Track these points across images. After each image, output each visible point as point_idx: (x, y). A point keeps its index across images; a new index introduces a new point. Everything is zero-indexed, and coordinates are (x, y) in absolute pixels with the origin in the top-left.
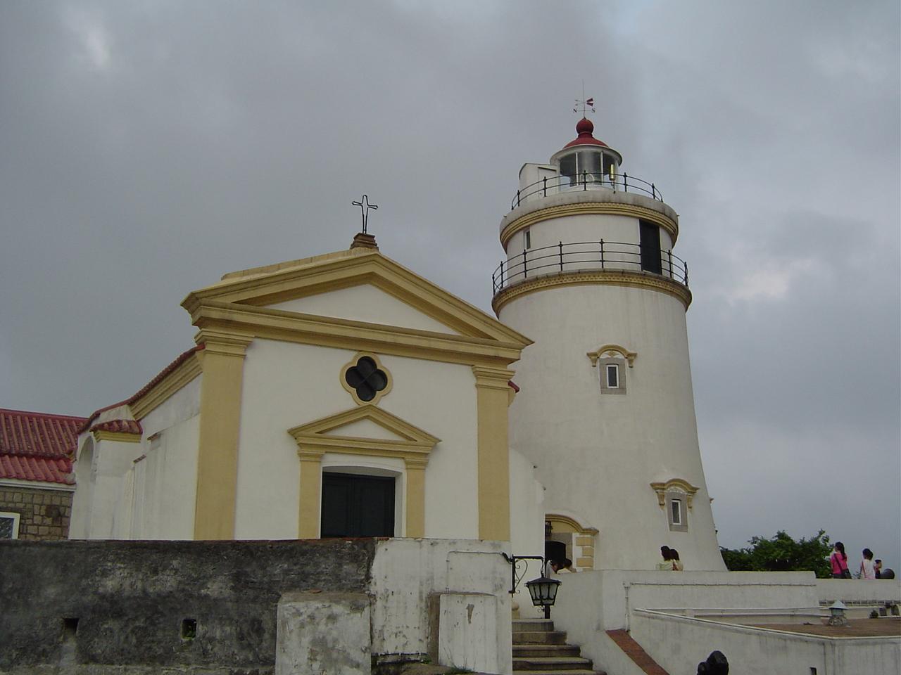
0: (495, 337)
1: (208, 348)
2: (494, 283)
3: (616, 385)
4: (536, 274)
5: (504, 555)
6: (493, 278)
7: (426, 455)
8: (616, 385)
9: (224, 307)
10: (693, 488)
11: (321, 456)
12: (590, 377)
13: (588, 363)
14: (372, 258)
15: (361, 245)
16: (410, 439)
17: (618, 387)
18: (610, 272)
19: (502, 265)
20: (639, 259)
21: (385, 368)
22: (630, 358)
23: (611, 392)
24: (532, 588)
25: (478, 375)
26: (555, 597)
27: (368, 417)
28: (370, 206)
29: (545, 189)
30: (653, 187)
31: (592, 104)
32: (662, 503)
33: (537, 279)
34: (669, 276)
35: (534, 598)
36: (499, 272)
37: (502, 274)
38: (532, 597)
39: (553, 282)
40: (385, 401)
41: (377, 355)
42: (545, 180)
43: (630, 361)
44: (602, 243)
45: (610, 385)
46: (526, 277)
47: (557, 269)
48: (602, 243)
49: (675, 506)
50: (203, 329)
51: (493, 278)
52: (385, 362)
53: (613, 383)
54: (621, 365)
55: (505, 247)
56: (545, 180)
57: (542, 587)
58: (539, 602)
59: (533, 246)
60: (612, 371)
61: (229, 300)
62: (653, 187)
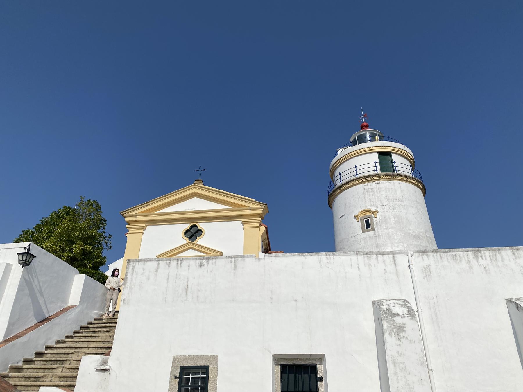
1: (130, 232)
9: (132, 216)
12: (358, 226)
17: (370, 228)
23: (368, 231)
25: (243, 224)
40: (200, 241)
45: (367, 228)
52: (201, 226)
53: (368, 226)
60: (367, 222)
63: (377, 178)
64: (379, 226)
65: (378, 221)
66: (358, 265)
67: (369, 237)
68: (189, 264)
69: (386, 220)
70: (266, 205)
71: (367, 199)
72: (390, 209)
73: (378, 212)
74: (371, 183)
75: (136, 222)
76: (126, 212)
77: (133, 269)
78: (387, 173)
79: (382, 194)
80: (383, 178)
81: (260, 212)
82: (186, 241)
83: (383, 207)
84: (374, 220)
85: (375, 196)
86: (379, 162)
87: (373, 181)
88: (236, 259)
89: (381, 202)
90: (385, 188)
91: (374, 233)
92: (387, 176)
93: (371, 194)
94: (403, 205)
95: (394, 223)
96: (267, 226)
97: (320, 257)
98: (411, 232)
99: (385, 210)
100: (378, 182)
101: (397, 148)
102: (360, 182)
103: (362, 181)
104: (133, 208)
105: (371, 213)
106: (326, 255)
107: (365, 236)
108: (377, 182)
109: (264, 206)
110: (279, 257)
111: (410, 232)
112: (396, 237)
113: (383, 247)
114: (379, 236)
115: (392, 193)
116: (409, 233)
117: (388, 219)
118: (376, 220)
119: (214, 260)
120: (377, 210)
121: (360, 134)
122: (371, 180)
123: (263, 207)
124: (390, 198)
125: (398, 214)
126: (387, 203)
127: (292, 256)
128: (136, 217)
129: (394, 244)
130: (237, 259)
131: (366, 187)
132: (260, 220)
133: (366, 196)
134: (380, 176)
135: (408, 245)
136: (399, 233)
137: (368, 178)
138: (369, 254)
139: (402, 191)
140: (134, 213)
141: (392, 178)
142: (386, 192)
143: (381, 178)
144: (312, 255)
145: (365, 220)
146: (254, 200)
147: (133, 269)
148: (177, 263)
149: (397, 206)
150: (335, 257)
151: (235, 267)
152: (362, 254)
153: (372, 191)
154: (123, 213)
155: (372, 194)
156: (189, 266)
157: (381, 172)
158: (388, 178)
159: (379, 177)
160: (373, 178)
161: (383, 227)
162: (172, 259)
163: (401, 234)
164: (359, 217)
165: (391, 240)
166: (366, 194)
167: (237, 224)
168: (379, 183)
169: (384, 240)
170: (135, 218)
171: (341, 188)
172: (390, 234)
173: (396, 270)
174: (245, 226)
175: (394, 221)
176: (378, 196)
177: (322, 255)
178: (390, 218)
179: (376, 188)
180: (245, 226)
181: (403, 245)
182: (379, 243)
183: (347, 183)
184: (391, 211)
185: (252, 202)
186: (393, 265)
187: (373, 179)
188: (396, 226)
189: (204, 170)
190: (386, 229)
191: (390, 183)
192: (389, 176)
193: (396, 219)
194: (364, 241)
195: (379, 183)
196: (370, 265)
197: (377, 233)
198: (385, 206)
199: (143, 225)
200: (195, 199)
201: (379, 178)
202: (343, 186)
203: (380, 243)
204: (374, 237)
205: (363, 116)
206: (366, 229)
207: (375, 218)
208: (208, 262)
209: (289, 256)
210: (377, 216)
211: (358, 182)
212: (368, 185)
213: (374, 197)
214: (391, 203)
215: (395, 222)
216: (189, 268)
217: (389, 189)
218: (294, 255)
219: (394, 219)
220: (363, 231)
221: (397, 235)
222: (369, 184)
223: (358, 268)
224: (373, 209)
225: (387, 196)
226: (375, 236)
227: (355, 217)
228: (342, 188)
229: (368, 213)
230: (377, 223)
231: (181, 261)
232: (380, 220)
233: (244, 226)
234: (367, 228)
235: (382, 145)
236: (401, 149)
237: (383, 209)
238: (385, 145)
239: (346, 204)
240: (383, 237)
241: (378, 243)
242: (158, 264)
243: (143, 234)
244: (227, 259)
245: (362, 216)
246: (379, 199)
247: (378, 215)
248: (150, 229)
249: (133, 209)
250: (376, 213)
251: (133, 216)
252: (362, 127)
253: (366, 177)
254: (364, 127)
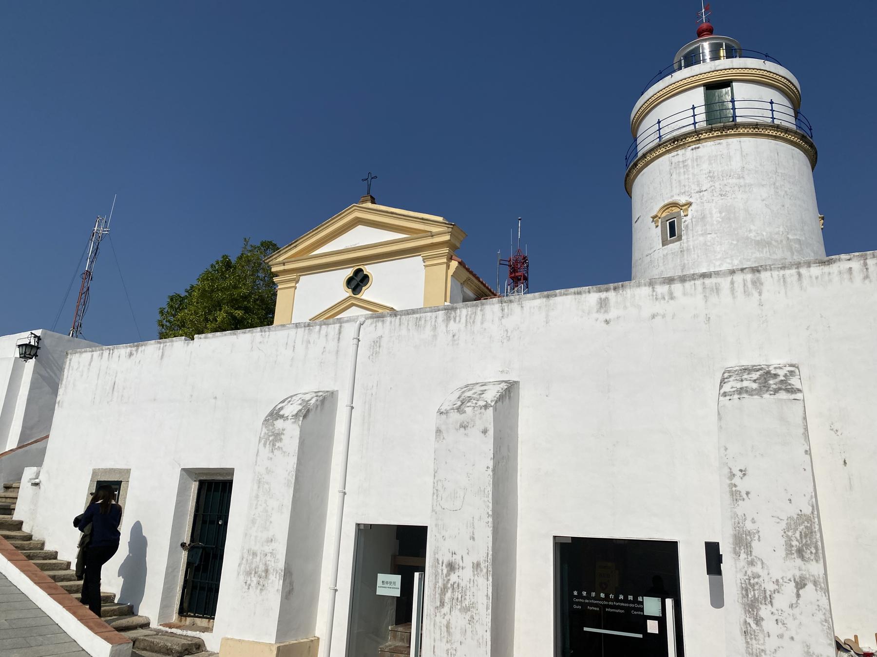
1: (279, 287)
23: (673, 242)
40: (367, 294)
45: (670, 238)
52: (368, 269)
53: (672, 234)
54: (678, 215)
60: (672, 225)
63: (694, 139)
64: (690, 232)
65: (690, 221)
66: (295, 343)
67: (672, 253)
68: (120, 354)
69: (703, 218)
70: (453, 225)
71: (674, 182)
72: (713, 195)
73: (690, 204)
74: (683, 151)
76: (271, 259)
77: (70, 363)
78: (713, 126)
79: (701, 168)
80: (707, 136)
81: (447, 238)
82: (348, 293)
83: (702, 194)
84: (683, 220)
85: (688, 175)
87: (687, 145)
88: (165, 344)
89: (698, 185)
90: (710, 157)
91: (681, 245)
92: (713, 132)
93: (682, 170)
94: (742, 184)
95: (719, 222)
96: (460, 260)
97: (254, 334)
98: (752, 235)
99: (705, 198)
100: (697, 146)
101: (746, 69)
102: (664, 150)
103: (668, 149)
104: (278, 252)
105: (679, 208)
106: (261, 331)
107: (665, 252)
108: (694, 146)
109: (452, 228)
110: (209, 338)
111: (749, 235)
112: (718, 249)
113: (693, 269)
114: (688, 250)
115: (721, 164)
116: (747, 238)
117: (709, 216)
118: (687, 220)
119: (143, 347)
120: (691, 200)
121: (688, 50)
122: (684, 144)
123: (450, 230)
124: (716, 174)
125: (728, 204)
126: (709, 186)
127: (223, 336)
128: (284, 265)
129: (714, 261)
130: (166, 344)
131: (675, 160)
132: (448, 251)
133: (674, 176)
134: (700, 134)
135: (740, 261)
136: (727, 240)
138: (311, 325)
139: (743, 156)
140: (281, 259)
141: (724, 133)
142: (710, 164)
143: (702, 137)
144: (245, 333)
145: (669, 223)
146: (440, 219)
147: (70, 363)
148: (109, 354)
149: (728, 189)
150: (271, 332)
151: (162, 355)
152: (303, 325)
153: (684, 166)
154: (268, 260)
155: (684, 172)
156: (119, 357)
158: (715, 134)
159: (698, 135)
160: (687, 139)
161: (697, 232)
162: (104, 348)
163: (730, 241)
164: (659, 218)
165: (709, 255)
166: (673, 172)
167: (417, 261)
168: (698, 148)
169: (696, 256)
170: (283, 266)
171: (636, 167)
172: (709, 244)
173: (338, 347)
174: (428, 263)
175: (718, 219)
176: (694, 175)
177: (256, 332)
178: (711, 213)
179: (693, 160)
180: (428, 263)
181: (730, 262)
182: (686, 262)
184: (714, 201)
185: (431, 222)
186: (336, 340)
187: (686, 142)
188: (721, 228)
190: (702, 235)
191: (720, 143)
192: (717, 131)
193: (724, 214)
194: (664, 262)
195: (698, 148)
196: (309, 342)
197: (685, 245)
198: (705, 191)
199: (294, 276)
200: (360, 228)
201: (698, 138)
202: (639, 162)
203: (688, 263)
204: (680, 252)
205: (703, 10)
206: (669, 239)
207: (685, 216)
208: (137, 350)
209: (220, 336)
210: (690, 213)
211: (661, 152)
212: (678, 155)
213: (686, 176)
214: (717, 185)
215: (721, 220)
216: (119, 360)
217: (716, 156)
218: (225, 335)
219: (719, 215)
221: (721, 245)
222: (680, 152)
223: (294, 347)
224: (682, 200)
225: (710, 172)
226: (681, 251)
227: (654, 218)
228: (637, 167)
229: (674, 208)
230: (687, 226)
231: (113, 350)
232: (693, 220)
234: (670, 238)
235: (713, 70)
236: (754, 69)
237: (699, 198)
238: (717, 69)
239: (643, 196)
240: (694, 251)
241: (684, 264)
242: (92, 356)
243: (296, 289)
244: (156, 346)
245: (664, 214)
246: (695, 180)
247: (691, 211)
248: (305, 280)
249: (279, 254)
250: (687, 206)
251: (280, 264)
252: (700, 34)
253: (675, 140)
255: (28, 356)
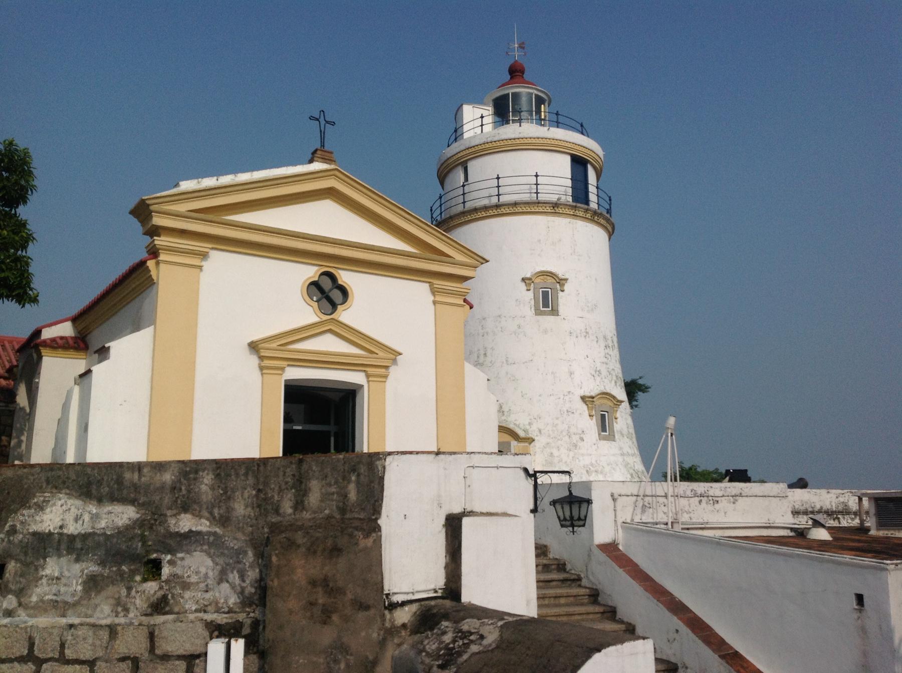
0: (451, 255)
1: (163, 257)
2: (432, 214)
3: (549, 308)
4: (474, 206)
5: (526, 470)
6: (431, 210)
7: (387, 367)
8: (549, 308)
10: (618, 401)
11: (283, 369)
13: (523, 286)
14: (331, 173)
15: (321, 160)
16: (372, 352)
18: (544, 203)
19: (440, 198)
20: (570, 191)
21: (348, 285)
22: (562, 282)
24: (558, 507)
25: (434, 292)
26: (586, 517)
27: (330, 331)
28: (327, 122)
29: (482, 125)
30: (582, 126)
31: (523, 48)
32: (591, 414)
33: (476, 210)
34: (597, 208)
35: (562, 518)
36: (438, 203)
37: (441, 206)
38: (559, 518)
39: (491, 212)
40: (346, 315)
41: (340, 271)
42: (482, 117)
43: (562, 285)
44: (537, 176)
46: (464, 208)
47: (494, 200)
48: (537, 176)
49: (603, 417)
50: (155, 238)
51: (431, 210)
52: (346, 277)
55: (442, 183)
56: (482, 117)
57: (573, 506)
58: (568, 523)
59: (470, 180)
60: (545, 295)
61: (182, 208)
62: (582, 126)
63: (572, 213)
75: (183, 233)
86: (571, 179)
137: (555, 208)
145: (542, 291)
157: (573, 201)
174: (438, 298)
180: (438, 298)
183: (515, 204)
189: (333, 124)
202: (504, 207)
220: (538, 312)
224: (560, 272)
227: (523, 280)
229: (549, 278)
233: (436, 299)
243: (201, 270)
254: (518, 72)
255: (564, 523)
